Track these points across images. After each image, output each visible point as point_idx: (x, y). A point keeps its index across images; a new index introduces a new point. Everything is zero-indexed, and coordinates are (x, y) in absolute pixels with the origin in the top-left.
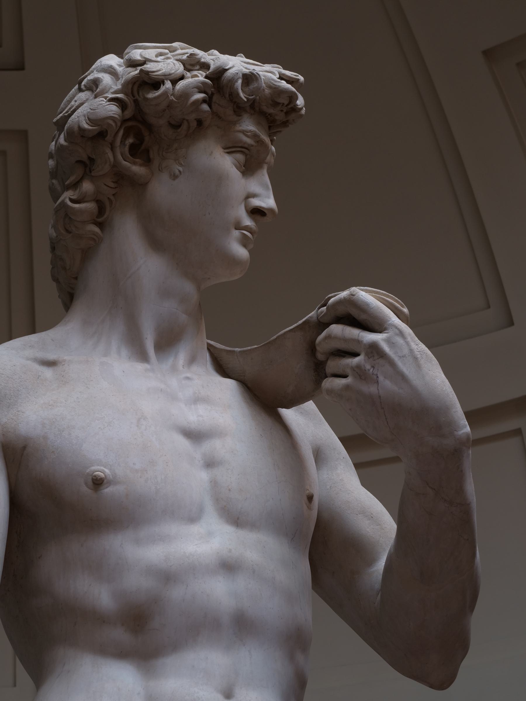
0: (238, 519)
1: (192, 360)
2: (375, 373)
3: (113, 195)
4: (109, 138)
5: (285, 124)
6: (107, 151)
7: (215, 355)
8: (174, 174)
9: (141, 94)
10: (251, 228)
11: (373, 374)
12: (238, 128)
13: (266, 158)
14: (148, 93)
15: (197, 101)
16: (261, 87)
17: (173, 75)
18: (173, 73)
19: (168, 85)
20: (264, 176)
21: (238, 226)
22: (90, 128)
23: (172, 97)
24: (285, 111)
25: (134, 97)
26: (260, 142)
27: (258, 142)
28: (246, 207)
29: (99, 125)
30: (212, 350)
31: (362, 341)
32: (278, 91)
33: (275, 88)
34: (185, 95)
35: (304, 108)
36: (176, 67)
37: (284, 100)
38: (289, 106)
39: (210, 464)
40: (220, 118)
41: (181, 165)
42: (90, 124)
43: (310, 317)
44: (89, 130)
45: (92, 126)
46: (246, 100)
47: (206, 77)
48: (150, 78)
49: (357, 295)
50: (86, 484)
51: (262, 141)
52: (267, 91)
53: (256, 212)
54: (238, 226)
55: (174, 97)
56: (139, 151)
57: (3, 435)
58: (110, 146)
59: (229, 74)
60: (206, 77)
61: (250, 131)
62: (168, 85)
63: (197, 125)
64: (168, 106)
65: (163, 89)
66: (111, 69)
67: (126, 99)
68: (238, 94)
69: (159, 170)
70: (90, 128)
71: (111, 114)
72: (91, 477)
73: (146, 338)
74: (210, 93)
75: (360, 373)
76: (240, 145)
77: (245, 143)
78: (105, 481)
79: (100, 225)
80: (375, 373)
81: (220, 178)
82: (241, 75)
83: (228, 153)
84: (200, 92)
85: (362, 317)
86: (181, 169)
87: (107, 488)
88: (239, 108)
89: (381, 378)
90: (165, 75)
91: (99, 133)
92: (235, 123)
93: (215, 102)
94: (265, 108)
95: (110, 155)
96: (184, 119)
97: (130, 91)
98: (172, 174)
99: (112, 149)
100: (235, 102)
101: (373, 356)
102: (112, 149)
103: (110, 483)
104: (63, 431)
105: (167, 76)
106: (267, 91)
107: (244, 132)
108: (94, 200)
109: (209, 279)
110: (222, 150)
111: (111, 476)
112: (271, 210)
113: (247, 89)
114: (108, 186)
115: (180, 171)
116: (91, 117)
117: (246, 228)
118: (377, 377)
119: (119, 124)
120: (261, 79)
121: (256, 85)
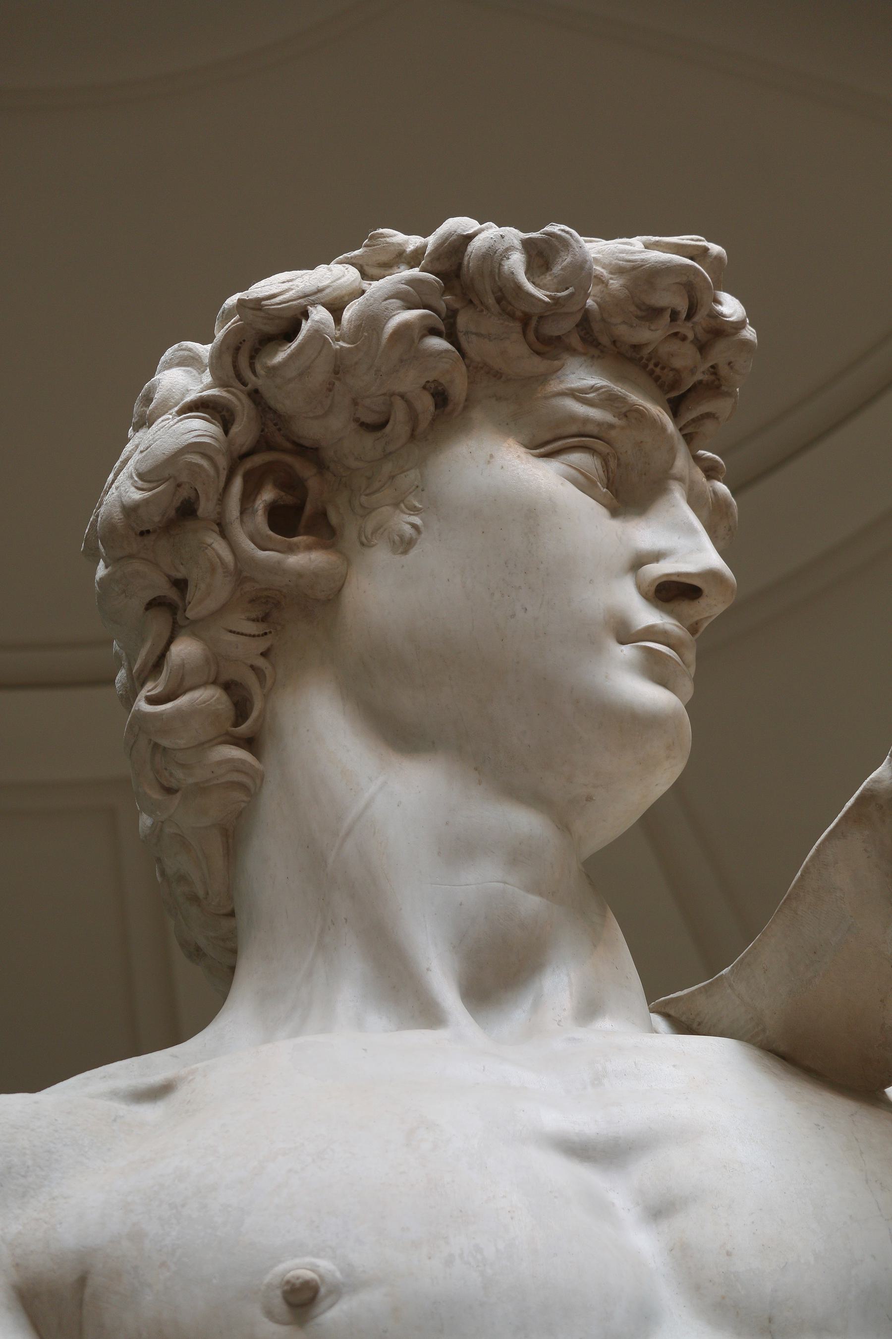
0: (770, 1320)
1: (590, 1009)
3: (264, 654)
4: (206, 507)
5: (714, 386)
6: (209, 540)
7: (683, 1019)
8: (401, 537)
9: (258, 367)
12: (555, 386)
13: (671, 465)
14: (276, 353)
15: (404, 329)
16: (585, 261)
17: (327, 291)
19: (320, 314)
21: (625, 634)
22: (147, 494)
23: (341, 343)
24: (691, 336)
25: (245, 384)
28: (639, 588)
30: (672, 1013)
32: (643, 276)
33: (634, 268)
34: (371, 322)
37: (671, 298)
38: (700, 317)
39: (659, 1210)
40: (497, 375)
41: (415, 510)
42: (146, 485)
43: (874, 781)
44: (146, 502)
45: (150, 490)
46: (547, 299)
50: (270, 1314)
51: (638, 411)
52: (615, 283)
53: (672, 593)
55: (344, 341)
57: (17, 1265)
58: (217, 528)
59: (476, 245)
61: (593, 389)
62: (320, 314)
63: (437, 406)
64: (336, 372)
65: (306, 326)
66: (181, 353)
67: (225, 394)
68: (519, 287)
69: (362, 544)
70: (147, 494)
71: (190, 438)
72: (279, 1292)
73: (428, 969)
74: (442, 306)
76: (574, 429)
77: (586, 420)
78: (323, 1290)
79: (251, 743)
81: (531, 514)
82: (517, 243)
87: (331, 1306)
90: (306, 296)
91: (178, 507)
92: (543, 378)
93: (467, 333)
94: (624, 332)
95: (220, 546)
96: (392, 395)
97: (232, 373)
98: (397, 538)
99: (223, 531)
100: (525, 320)
102: (223, 533)
103: (337, 1291)
104: (183, 1206)
105: (313, 297)
106: (615, 283)
107: (575, 394)
108: (214, 683)
109: (589, 799)
110: (524, 449)
111: (338, 1275)
112: (712, 575)
113: (548, 279)
114: (238, 633)
115: (414, 526)
116: (143, 468)
119: (223, 462)
121: (569, 259)
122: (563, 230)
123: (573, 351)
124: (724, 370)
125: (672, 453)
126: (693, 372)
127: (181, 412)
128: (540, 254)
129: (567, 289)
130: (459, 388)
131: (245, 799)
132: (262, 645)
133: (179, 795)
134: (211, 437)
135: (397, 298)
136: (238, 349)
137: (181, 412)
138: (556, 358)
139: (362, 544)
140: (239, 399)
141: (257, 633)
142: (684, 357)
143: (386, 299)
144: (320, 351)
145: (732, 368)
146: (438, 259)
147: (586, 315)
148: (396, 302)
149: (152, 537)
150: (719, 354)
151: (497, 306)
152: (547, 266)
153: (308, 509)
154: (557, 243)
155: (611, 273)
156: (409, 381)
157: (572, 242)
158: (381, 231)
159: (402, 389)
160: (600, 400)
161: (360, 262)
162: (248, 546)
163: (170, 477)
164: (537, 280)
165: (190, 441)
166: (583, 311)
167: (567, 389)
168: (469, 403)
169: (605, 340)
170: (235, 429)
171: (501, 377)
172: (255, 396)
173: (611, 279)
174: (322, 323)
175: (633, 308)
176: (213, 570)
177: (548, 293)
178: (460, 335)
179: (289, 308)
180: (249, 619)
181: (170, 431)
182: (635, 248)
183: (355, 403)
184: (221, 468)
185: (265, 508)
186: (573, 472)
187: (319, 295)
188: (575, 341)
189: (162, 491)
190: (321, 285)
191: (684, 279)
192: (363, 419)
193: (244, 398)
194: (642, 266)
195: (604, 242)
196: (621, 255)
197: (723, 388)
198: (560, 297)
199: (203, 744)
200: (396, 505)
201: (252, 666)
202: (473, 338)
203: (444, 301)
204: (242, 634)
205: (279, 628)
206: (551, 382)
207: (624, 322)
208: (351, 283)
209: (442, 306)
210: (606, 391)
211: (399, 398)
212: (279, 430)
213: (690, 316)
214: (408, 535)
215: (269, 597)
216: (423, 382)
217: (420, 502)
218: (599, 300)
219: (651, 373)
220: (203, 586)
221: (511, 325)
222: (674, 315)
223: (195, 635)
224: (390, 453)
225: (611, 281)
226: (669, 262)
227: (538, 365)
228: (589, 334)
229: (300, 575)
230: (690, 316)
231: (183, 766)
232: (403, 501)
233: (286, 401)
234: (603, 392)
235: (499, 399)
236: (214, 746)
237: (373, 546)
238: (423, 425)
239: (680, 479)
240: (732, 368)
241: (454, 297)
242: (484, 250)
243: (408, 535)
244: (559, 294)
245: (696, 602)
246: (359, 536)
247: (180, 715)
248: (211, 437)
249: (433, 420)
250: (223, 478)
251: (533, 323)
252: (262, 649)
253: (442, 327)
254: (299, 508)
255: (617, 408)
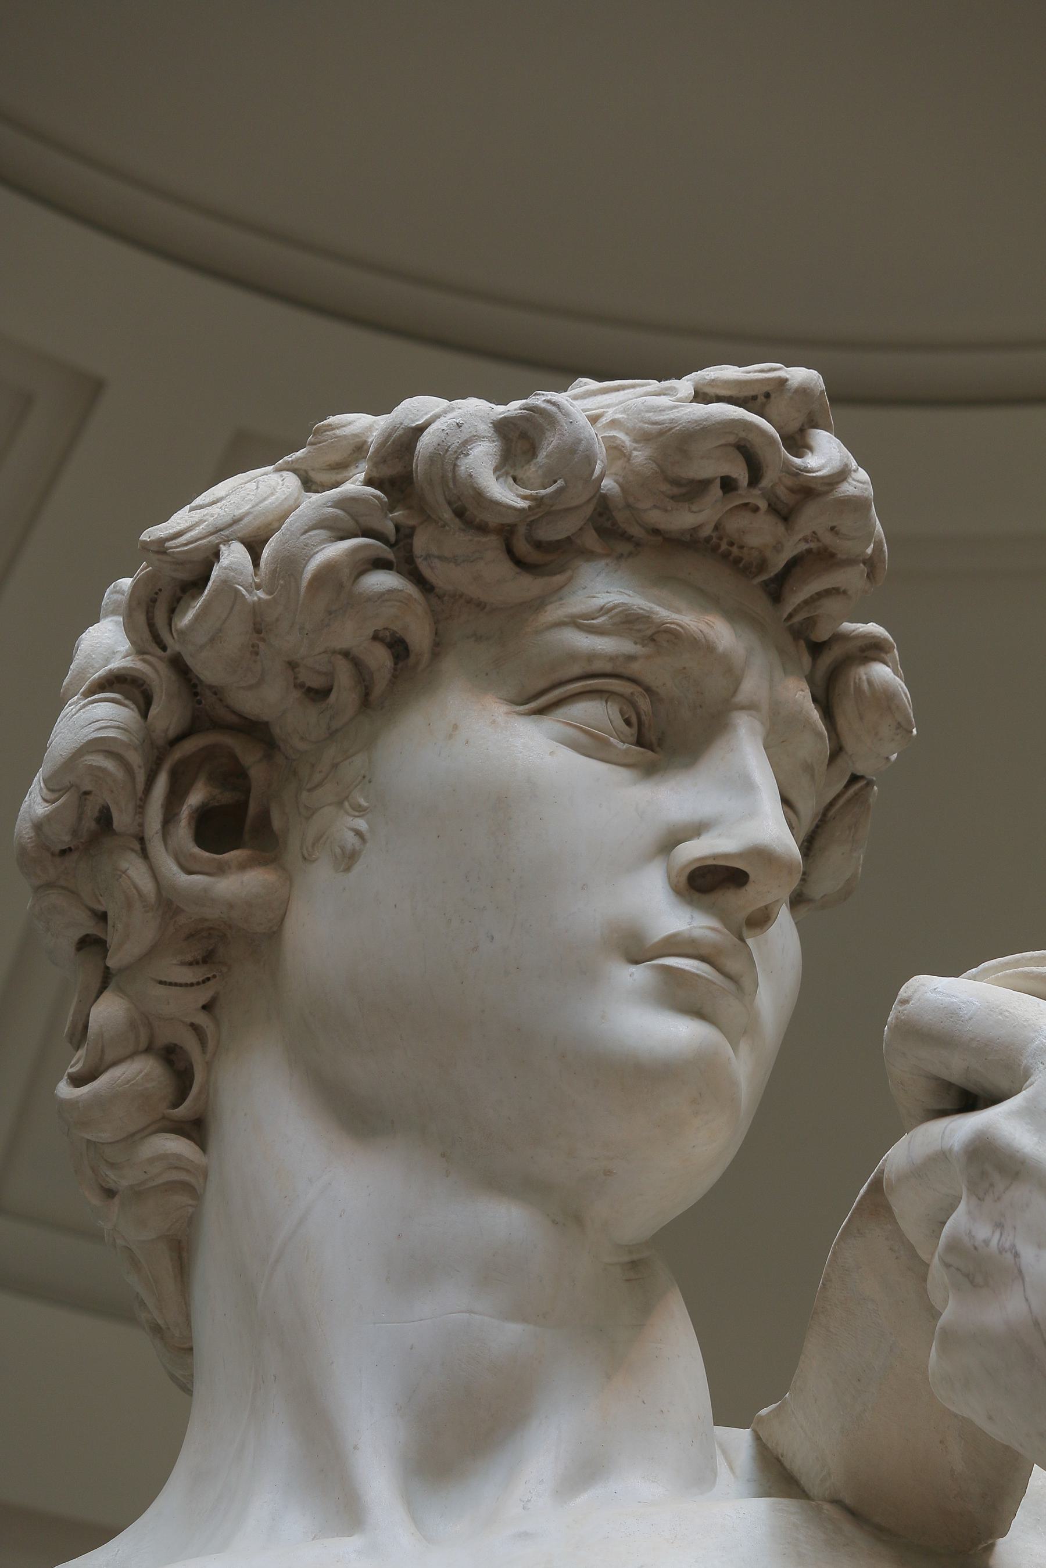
1: (586, 1471)
2: (1007, 1245)
4: (122, 819)
5: (820, 558)
10: (693, 942)
11: (1001, 1250)
12: (554, 612)
15: (328, 570)
17: (246, 520)
18: (247, 514)
20: (747, 751)
24: (763, 505)
25: (164, 648)
26: (660, 638)
27: (652, 639)
29: (67, 789)
31: (950, 1150)
32: (674, 442)
33: (661, 433)
34: (289, 565)
35: (862, 475)
36: (263, 489)
40: (480, 606)
41: (360, 811)
47: (369, 482)
48: (179, 562)
49: (916, 996)
51: (668, 631)
52: (640, 456)
54: (635, 948)
56: (231, 826)
59: (426, 440)
60: (369, 482)
61: (603, 610)
62: (234, 555)
67: (140, 665)
68: (479, 496)
69: (305, 858)
73: (355, 1448)
74: (389, 528)
75: (978, 1271)
76: (576, 670)
79: (196, 1129)
80: (1007, 1245)
82: (485, 428)
83: (541, 711)
84: (342, 539)
85: (955, 1068)
86: (362, 824)
88: (537, 548)
89: (1028, 1254)
92: (539, 604)
93: (428, 557)
94: (655, 517)
95: (136, 871)
96: (334, 652)
97: (146, 634)
98: (338, 850)
101: (992, 1185)
105: (224, 532)
107: (576, 622)
108: (148, 1050)
110: (504, 708)
112: (762, 855)
113: (531, 471)
114: (171, 984)
115: (358, 833)
117: (674, 945)
118: (1016, 1255)
119: (135, 759)
120: (567, 415)
122: (548, 401)
123: (588, 555)
124: (828, 539)
125: (734, 676)
126: (778, 548)
127: (91, 692)
128: (524, 436)
129: (555, 482)
130: (419, 634)
131: (191, 1202)
132: (203, 996)
133: (116, 1200)
134: (118, 728)
135: (321, 528)
136: (154, 601)
137: (91, 692)
138: (561, 570)
139: (305, 858)
140: (157, 671)
141: (194, 981)
142: (759, 532)
143: (306, 532)
144: (232, 608)
145: (837, 533)
146: (384, 461)
147: (603, 505)
148: (322, 534)
149: (75, 856)
150: (812, 520)
151: (457, 520)
152: (532, 451)
153: (253, 809)
154: (541, 420)
155: (636, 441)
156: (350, 634)
157: (560, 417)
158: (332, 420)
159: (343, 644)
160: (614, 624)
161: (304, 467)
162: (169, 867)
163: (72, 786)
164: (520, 473)
165: (89, 737)
166: (595, 501)
167: (566, 616)
168: (438, 649)
169: (635, 531)
170: (154, 711)
171: (484, 608)
172: (179, 666)
173: (635, 449)
174: (233, 570)
175: (665, 487)
176: (129, 905)
177: (528, 492)
178: (419, 561)
179: (196, 549)
180: (183, 964)
181: (70, 723)
182: (668, 401)
183: (292, 665)
184: (135, 767)
185: (191, 817)
186: (571, 731)
187: (235, 527)
188: (591, 540)
189: (63, 805)
190: (238, 513)
191: (732, 439)
192: (308, 684)
193: (163, 668)
194: (671, 429)
195: (654, 385)
196: (648, 415)
197: (839, 556)
198: (542, 497)
199: (133, 1135)
200: (340, 804)
201: (192, 1025)
202: (436, 563)
203: (392, 519)
204: (176, 985)
205: (225, 969)
206: (549, 608)
207: (655, 507)
208: (281, 504)
209: (389, 528)
210: (621, 612)
211: (340, 657)
212: (221, 700)
213: (754, 479)
214: (349, 847)
215: (211, 928)
216: (370, 632)
217: (366, 798)
218: (621, 480)
219: (726, 556)
220: (120, 926)
221: (484, 539)
222: (728, 485)
223: (121, 991)
224: (337, 731)
225: (635, 453)
226: (706, 420)
227: (527, 586)
228: (611, 529)
229: (231, 906)
230: (754, 479)
231: (112, 1166)
232: (347, 798)
233: (208, 669)
234: (617, 614)
235: (478, 638)
236: (142, 1138)
237: (316, 860)
238: (379, 687)
239: (750, 707)
240: (837, 533)
241: (406, 512)
242: (431, 449)
243: (349, 847)
244: (543, 492)
245: (743, 890)
246: (301, 848)
247: (98, 1102)
248: (118, 728)
249: (395, 676)
250: (141, 778)
251: (522, 530)
252: (203, 1001)
253: (388, 553)
254: (241, 807)
255: (639, 631)
